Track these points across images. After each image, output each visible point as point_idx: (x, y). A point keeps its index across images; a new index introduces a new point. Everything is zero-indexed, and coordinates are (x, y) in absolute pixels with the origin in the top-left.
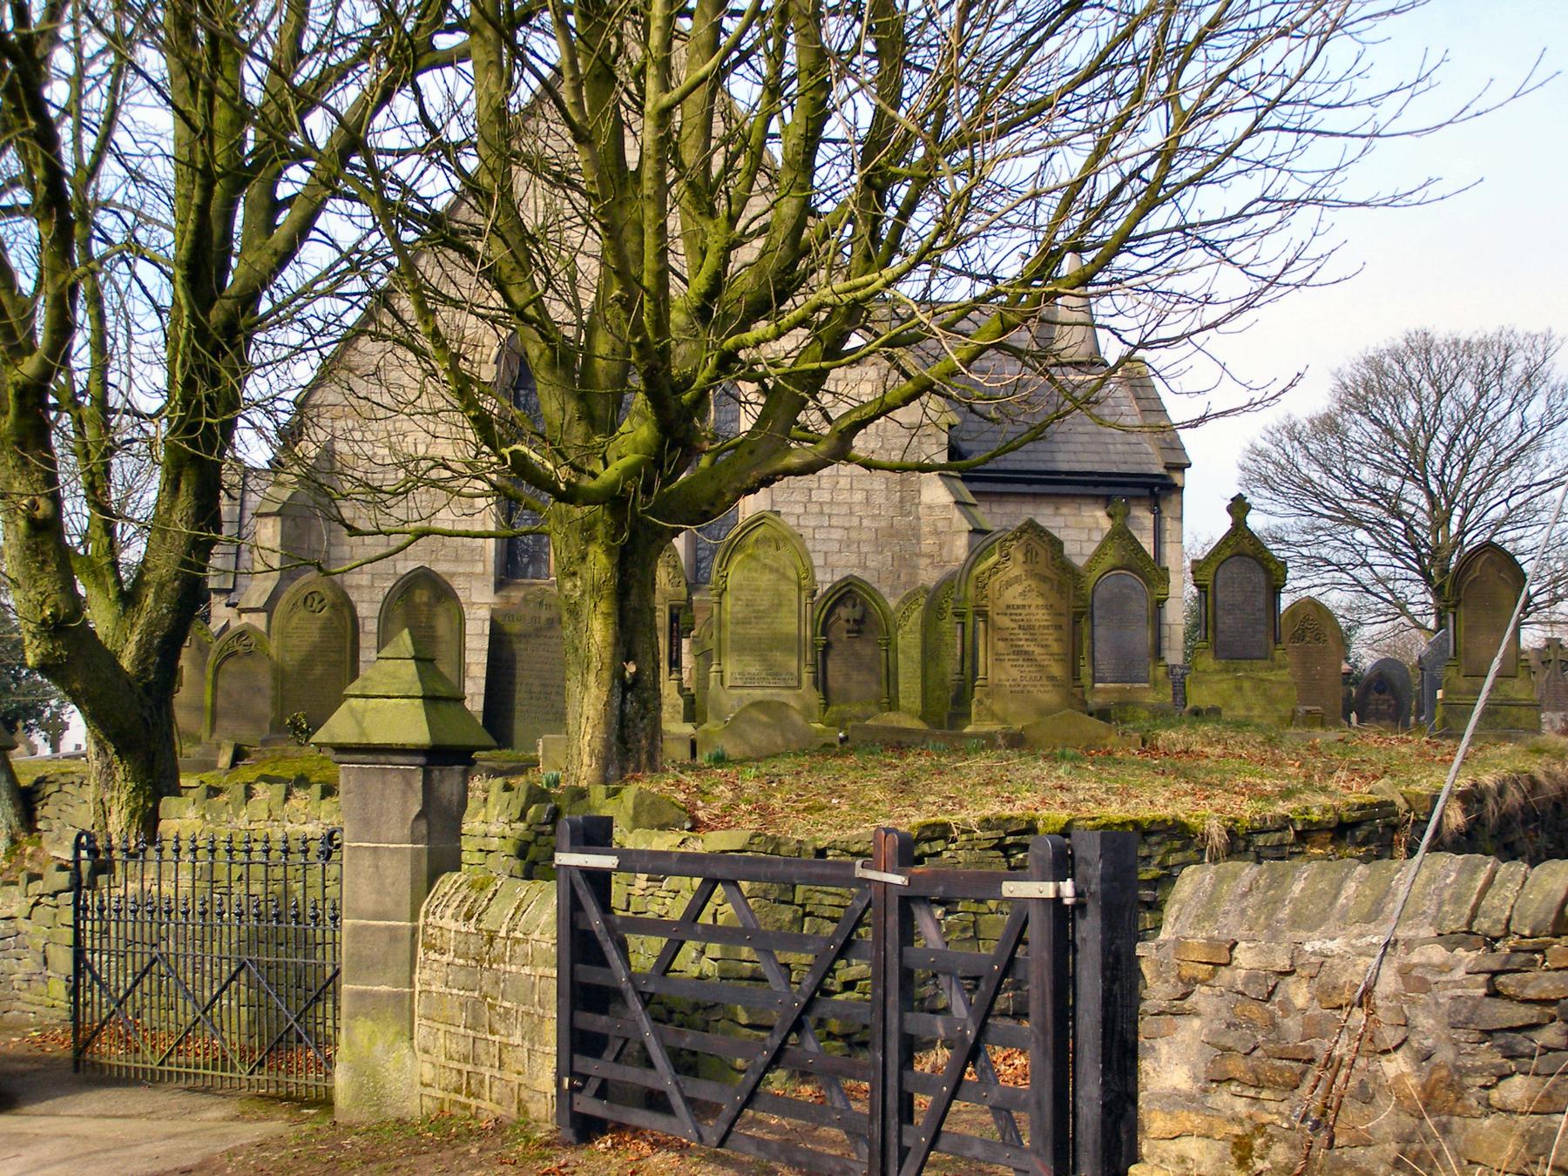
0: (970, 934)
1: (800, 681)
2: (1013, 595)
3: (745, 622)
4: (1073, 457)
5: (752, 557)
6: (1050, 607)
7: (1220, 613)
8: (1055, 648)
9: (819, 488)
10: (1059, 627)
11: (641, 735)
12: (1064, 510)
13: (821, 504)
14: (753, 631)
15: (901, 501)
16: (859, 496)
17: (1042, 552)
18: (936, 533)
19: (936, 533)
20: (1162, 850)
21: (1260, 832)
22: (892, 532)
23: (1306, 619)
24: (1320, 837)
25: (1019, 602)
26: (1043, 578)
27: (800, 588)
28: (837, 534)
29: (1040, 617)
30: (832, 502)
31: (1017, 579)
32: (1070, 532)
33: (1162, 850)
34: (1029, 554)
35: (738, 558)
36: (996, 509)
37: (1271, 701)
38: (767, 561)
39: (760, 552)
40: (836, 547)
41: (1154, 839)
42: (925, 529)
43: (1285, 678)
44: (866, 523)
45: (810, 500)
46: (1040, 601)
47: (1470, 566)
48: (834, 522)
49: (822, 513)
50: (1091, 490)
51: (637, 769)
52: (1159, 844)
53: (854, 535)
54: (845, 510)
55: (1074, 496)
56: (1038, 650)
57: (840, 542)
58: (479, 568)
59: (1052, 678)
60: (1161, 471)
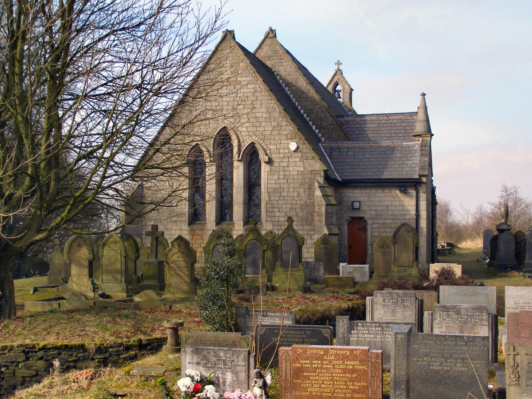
0: (12, 375)
1: (121, 281)
2: (175, 258)
3: (107, 265)
4: (389, 173)
5: (110, 247)
6: (185, 261)
7: (283, 253)
8: (187, 273)
9: (284, 191)
10: (187, 267)
11: (7, 310)
12: (386, 191)
13: (284, 197)
14: (110, 268)
15: (309, 195)
16: (296, 194)
17: (183, 246)
18: (318, 205)
19: (318, 205)
20: (76, 353)
21: (111, 347)
22: (306, 205)
23: (384, 241)
24: (135, 348)
25: (177, 260)
26: (183, 253)
27: (121, 256)
28: (289, 206)
29: (183, 264)
30: (287, 196)
31: (176, 253)
32: (388, 198)
33: (76, 353)
34: (179, 245)
35: (106, 247)
36: (363, 191)
37: (296, 281)
38: (113, 248)
39: (111, 245)
40: (289, 210)
41: (73, 350)
42: (316, 204)
43: (301, 274)
44: (298, 202)
45: (281, 196)
46: (182, 259)
47: (399, 232)
48: (288, 202)
49: (284, 199)
50: (394, 184)
51: (5, 318)
52: (75, 351)
53: (294, 206)
54: (291, 198)
55: (389, 186)
56: (182, 274)
57: (290, 208)
58: (184, 219)
59: (186, 282)
60: (417, 177)
